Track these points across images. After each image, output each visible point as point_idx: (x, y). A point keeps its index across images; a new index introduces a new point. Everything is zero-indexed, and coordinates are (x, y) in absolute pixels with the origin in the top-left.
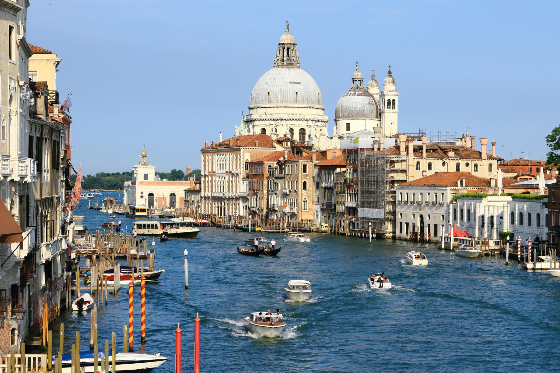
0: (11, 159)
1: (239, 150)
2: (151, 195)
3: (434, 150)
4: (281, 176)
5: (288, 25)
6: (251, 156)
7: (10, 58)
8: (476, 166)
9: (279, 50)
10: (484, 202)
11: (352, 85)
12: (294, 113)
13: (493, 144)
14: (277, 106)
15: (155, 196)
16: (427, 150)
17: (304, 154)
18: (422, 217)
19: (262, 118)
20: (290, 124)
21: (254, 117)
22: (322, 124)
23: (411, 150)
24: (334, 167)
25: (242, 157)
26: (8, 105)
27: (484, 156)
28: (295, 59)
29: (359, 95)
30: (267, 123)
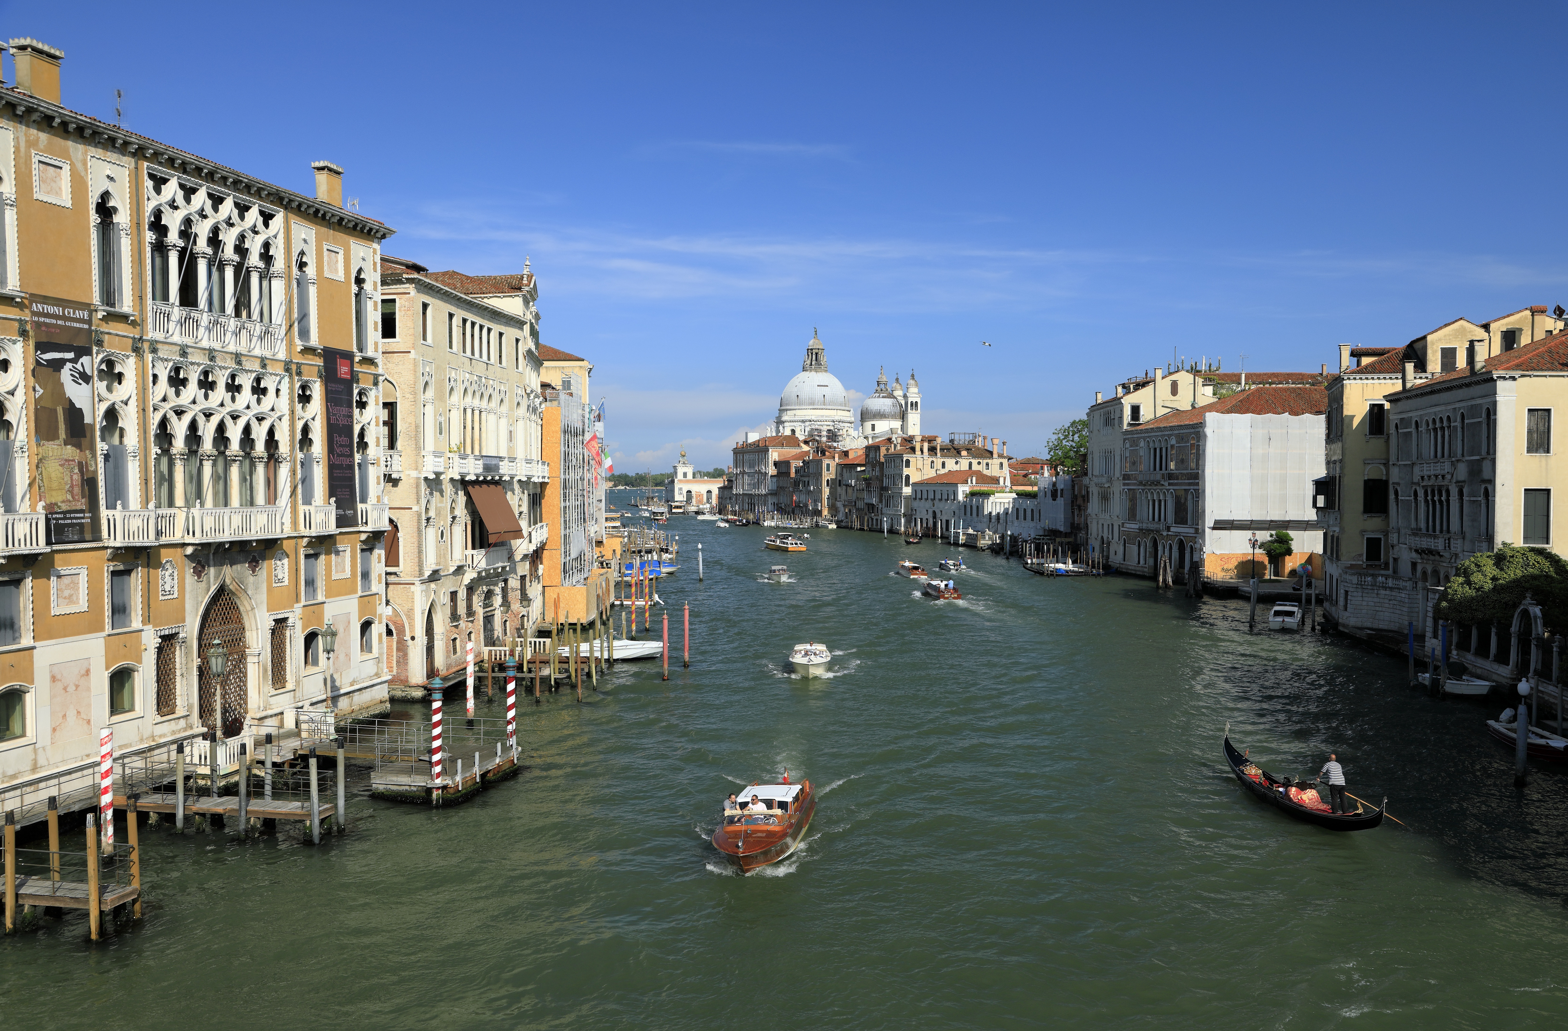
0: (517, 461)
3: (948, 449)
6: (779, 456)
8: (987, 464)
10: (992, 499)
13: (1004, 443)
16: (942, 450)
17: (827, 453)
18: (934, 512)
21: (784, 418)
22: (849, 425)
23: (926, 449)
27: (995, 456)
29: (883, 397)
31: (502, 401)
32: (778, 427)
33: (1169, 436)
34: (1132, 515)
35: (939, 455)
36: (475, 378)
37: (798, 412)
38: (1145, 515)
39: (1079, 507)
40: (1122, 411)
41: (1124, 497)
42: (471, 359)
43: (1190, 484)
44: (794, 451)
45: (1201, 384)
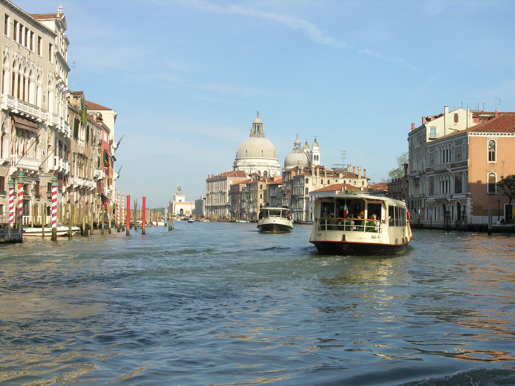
1: (226, 179)
2: (181, 210)
4: (248, 192)
5: (258, 113)
6: (233, 182)
7: (50, 60)
8: (355, 182)
9: (253, 127)
11: (293, 147)
12: (261, 162)
13: (365, 170)
14: (251, 158)
15: (184, 210)
17: (261, 179)
19: (243, 165)
20: (259, 168)
21: (238, 164)
24: (276, 185)
25: (228, 182)
26: (48, 85)
27: (359, 177)
28: (262, 132)
29: (298, 153)
30: (246, 167)
31: (38, 76)
32: (234, 170)
33: (452, 141)
34: (432, 193)
35: (326, 176)
36: (21, 57)
37: (247, 161)
38: (439, 191)
39: (404, 195)
40: (425, 131)
41: (427, 182)
42: (19, 45)
43: (463, 169)
44: (242, 179)
45: (471, 116)
